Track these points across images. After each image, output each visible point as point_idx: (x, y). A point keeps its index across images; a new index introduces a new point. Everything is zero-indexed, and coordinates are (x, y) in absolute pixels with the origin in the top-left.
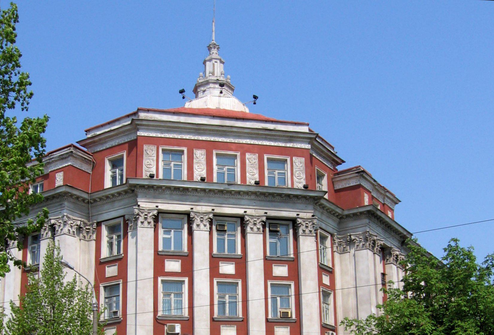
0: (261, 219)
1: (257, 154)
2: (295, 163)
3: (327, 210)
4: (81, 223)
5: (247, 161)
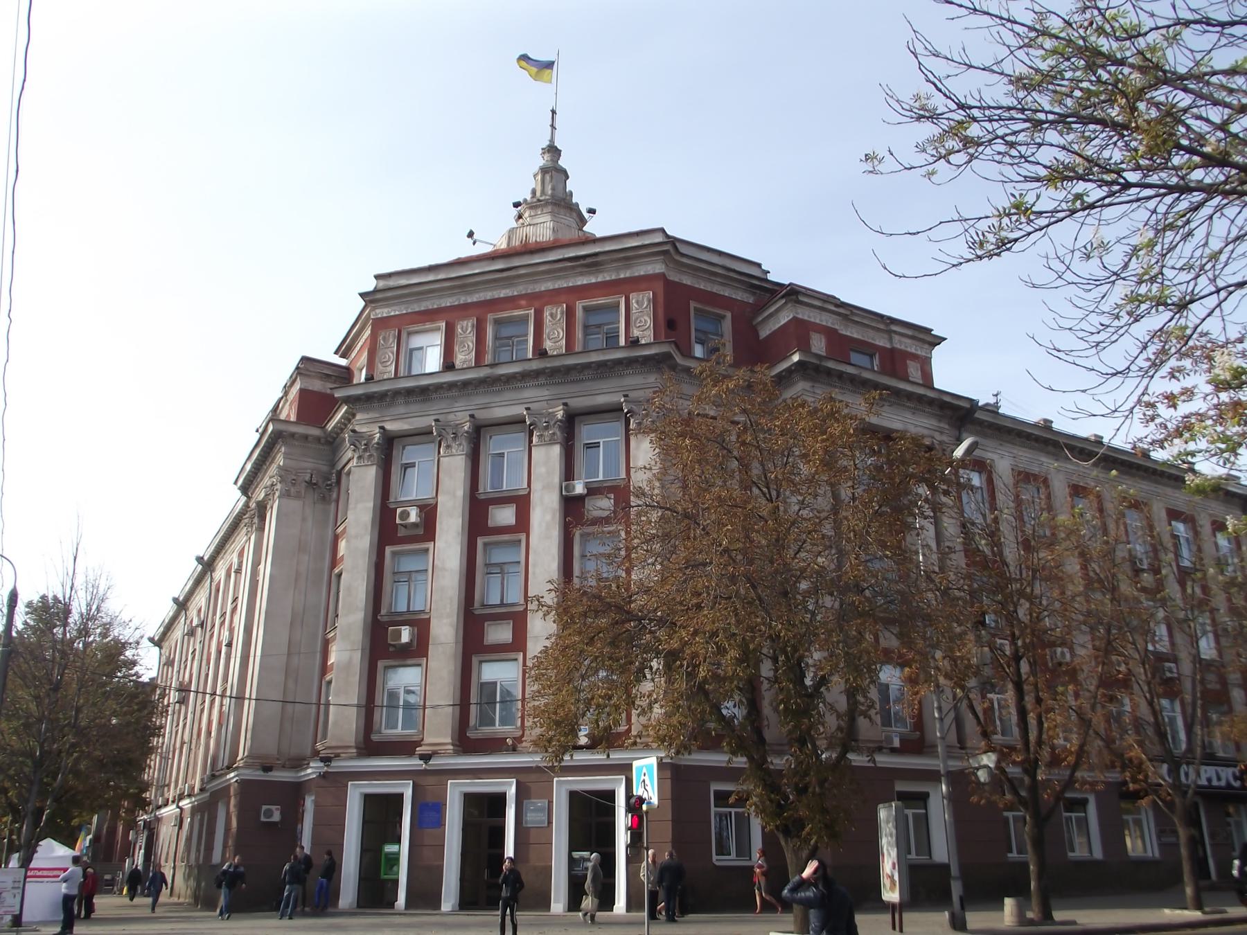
4: (311, 477)
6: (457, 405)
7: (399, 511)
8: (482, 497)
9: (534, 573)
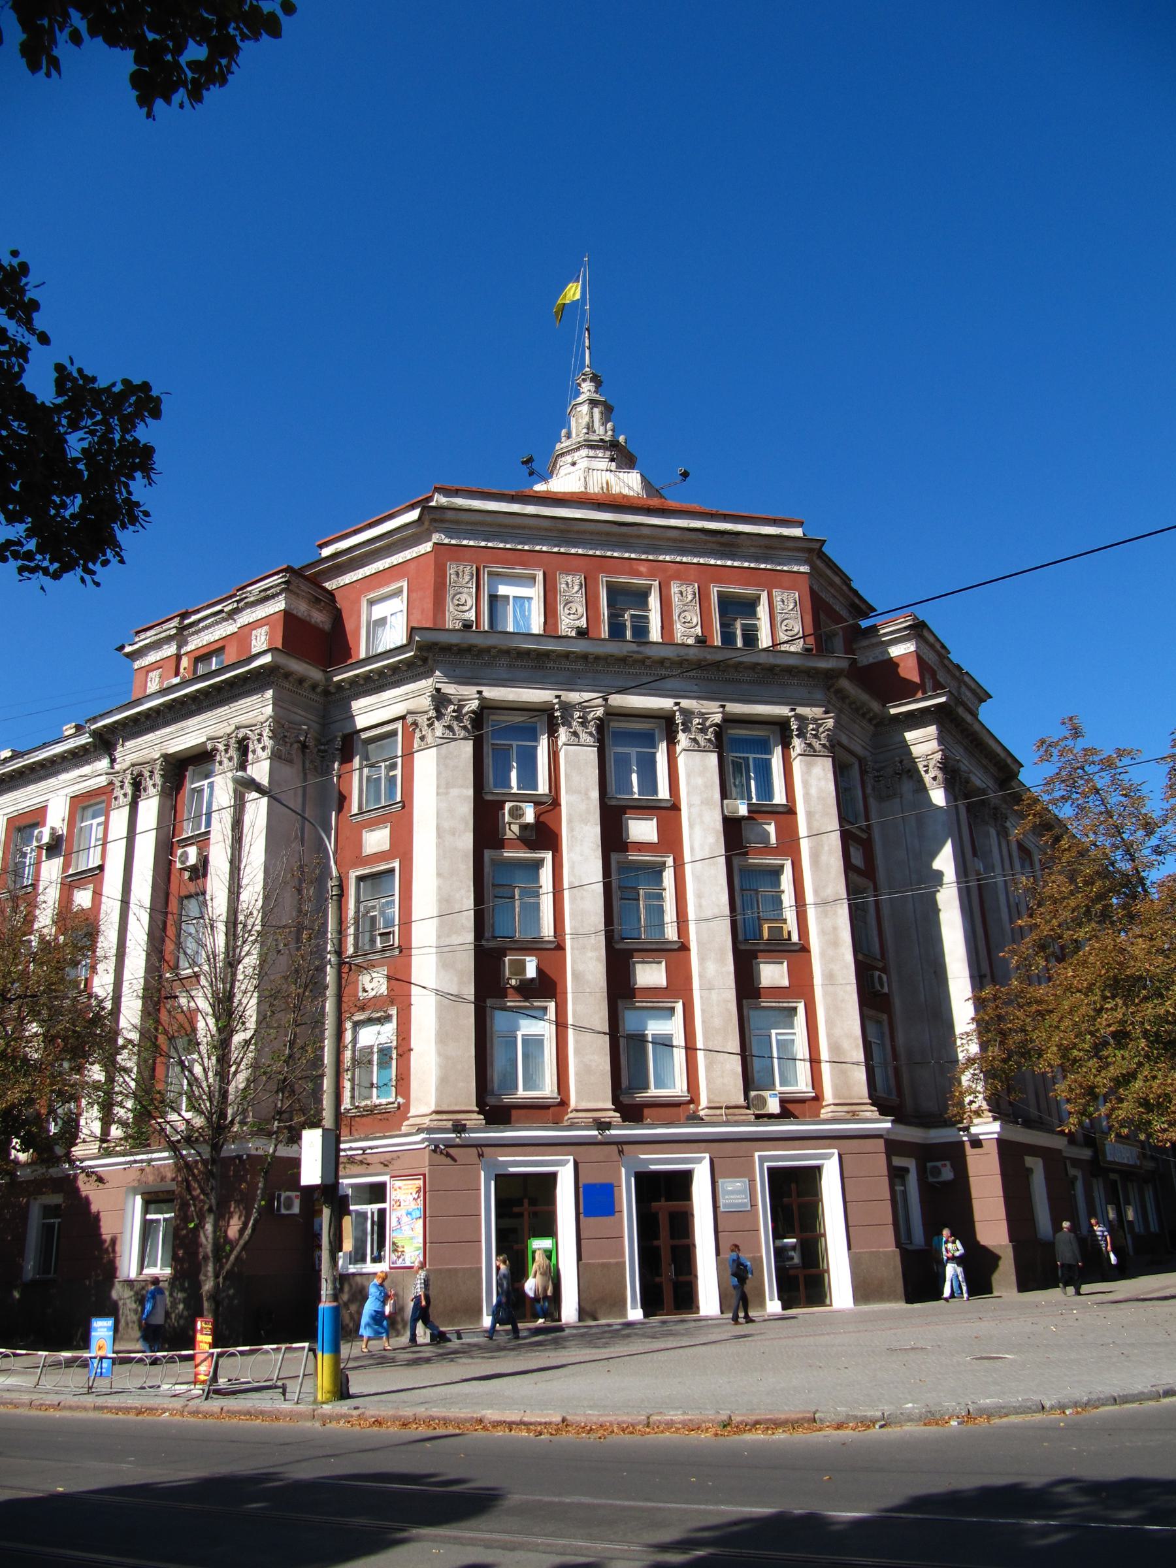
3: (850, 704)
7: (508, 806)
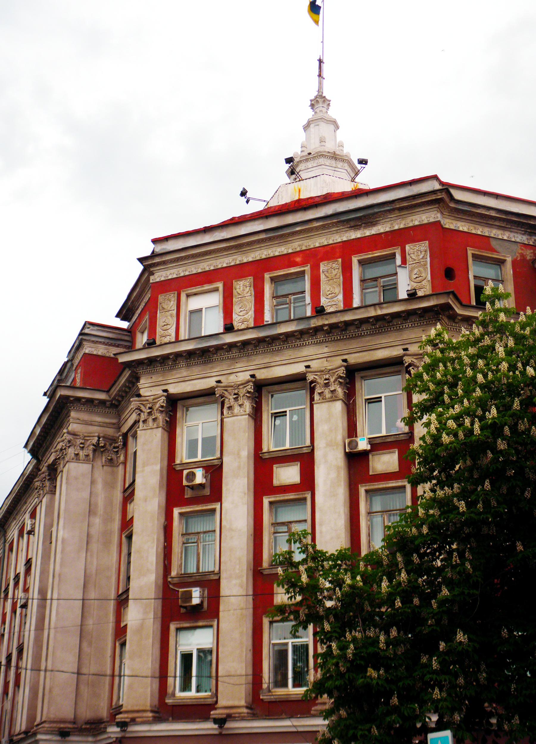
0: (337, 373)
1: (340, 260)
2: (409, 254)
4: (99, 440)
5: (322, 277)
6: (238, 365)
7: (185, 472)
8: (266, 456)
9: (321, 532)
